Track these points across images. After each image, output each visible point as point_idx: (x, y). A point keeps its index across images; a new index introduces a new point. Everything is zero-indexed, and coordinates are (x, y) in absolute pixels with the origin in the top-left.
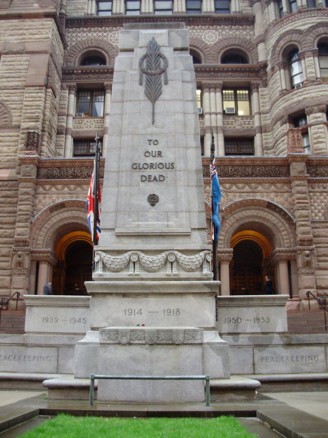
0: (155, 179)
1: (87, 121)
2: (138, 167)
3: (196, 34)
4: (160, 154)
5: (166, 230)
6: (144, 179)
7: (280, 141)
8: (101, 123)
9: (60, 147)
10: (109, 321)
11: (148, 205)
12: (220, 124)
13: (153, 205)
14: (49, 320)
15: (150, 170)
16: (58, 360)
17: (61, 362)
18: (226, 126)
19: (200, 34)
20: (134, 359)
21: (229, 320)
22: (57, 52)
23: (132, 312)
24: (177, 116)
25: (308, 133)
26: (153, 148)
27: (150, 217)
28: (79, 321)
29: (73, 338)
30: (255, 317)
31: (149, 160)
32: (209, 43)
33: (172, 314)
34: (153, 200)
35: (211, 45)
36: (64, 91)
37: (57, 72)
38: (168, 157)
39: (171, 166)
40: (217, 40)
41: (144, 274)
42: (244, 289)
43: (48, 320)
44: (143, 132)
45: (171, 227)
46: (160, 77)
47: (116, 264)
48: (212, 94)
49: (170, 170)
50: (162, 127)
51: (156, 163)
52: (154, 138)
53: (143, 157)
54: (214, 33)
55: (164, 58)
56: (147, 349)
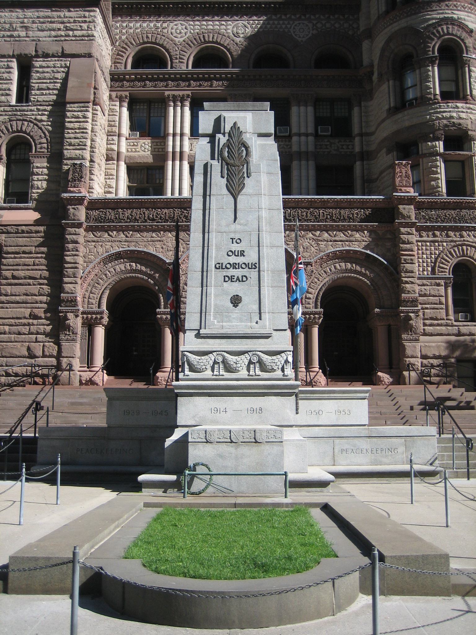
1: (144, 143)
3: (284, 26)
4: (242, 253)
5: (249, 331)
7: (385, 173)
8: (161, 145)
9: (111, 177)
12: (311, 148)
18: (318, 150)
19: (289, 26)
20: (221, 456)
21: (310, 412)
22: (103, 53)
25: (419, 165)
26: (235, 247)
27: (234, 318)
30: (336, 409)
31: (233, 259)
32: (300, 39)
33: (255, 412)
35: (302, 41)
36: (114, 103)
37: (105, 79)
39: (253, 267)
40: (310, 35)
42: (336, 353)
44: (226, 229)
45: (254, 328)
48: (302, 109)
50: (246, 225)
51: (239, 263)
54: (307, 25)
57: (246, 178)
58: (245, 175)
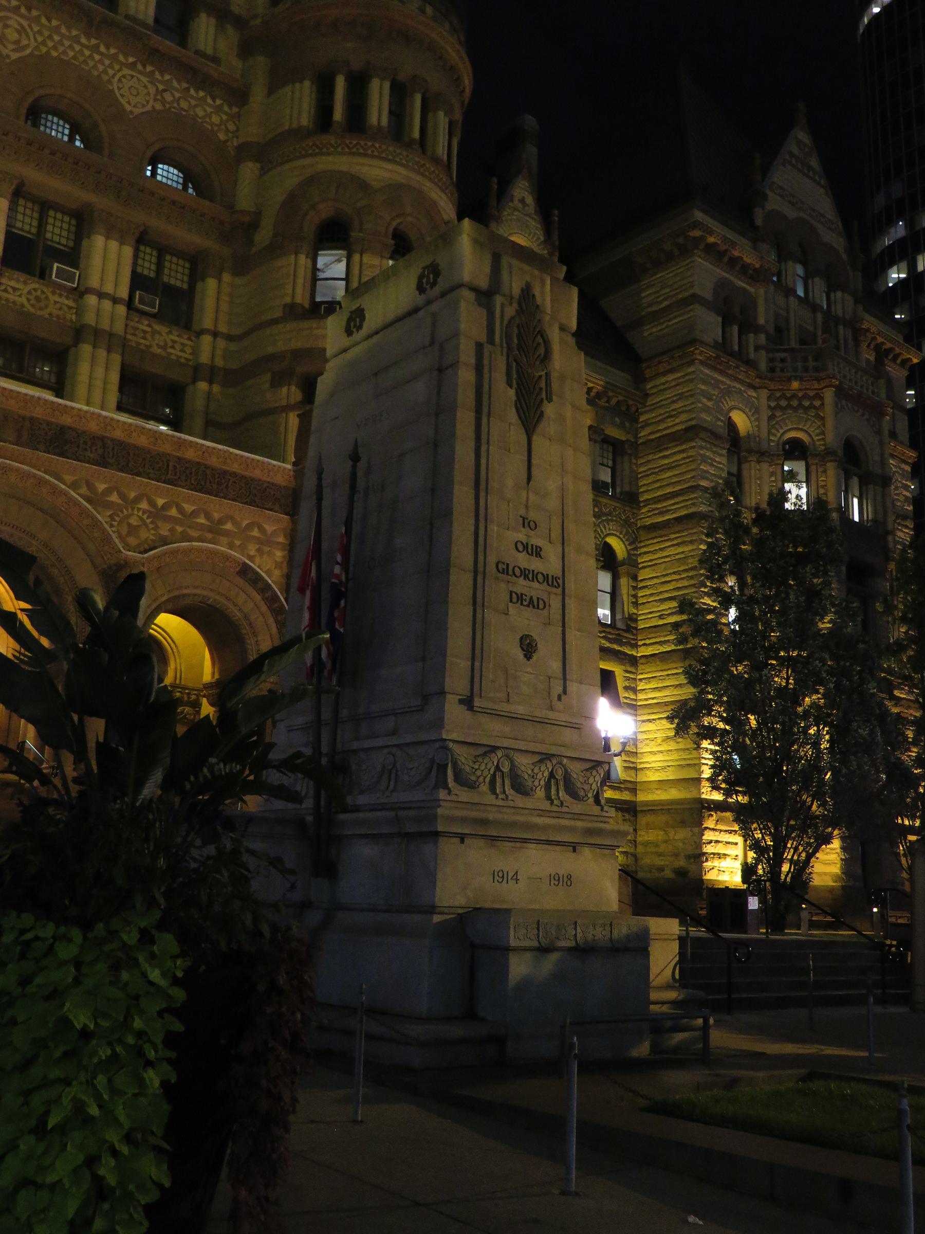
11: (520, 655)
12: (119, 328)
23: (503, 877)
32: (128, 108)
34: (528, 647)
35: (131, 112)
39: (555, 583)
40: (148, 108)
48: (113, 245)
54: (145, 87)
57: (545, 402)
58: (544, 395)
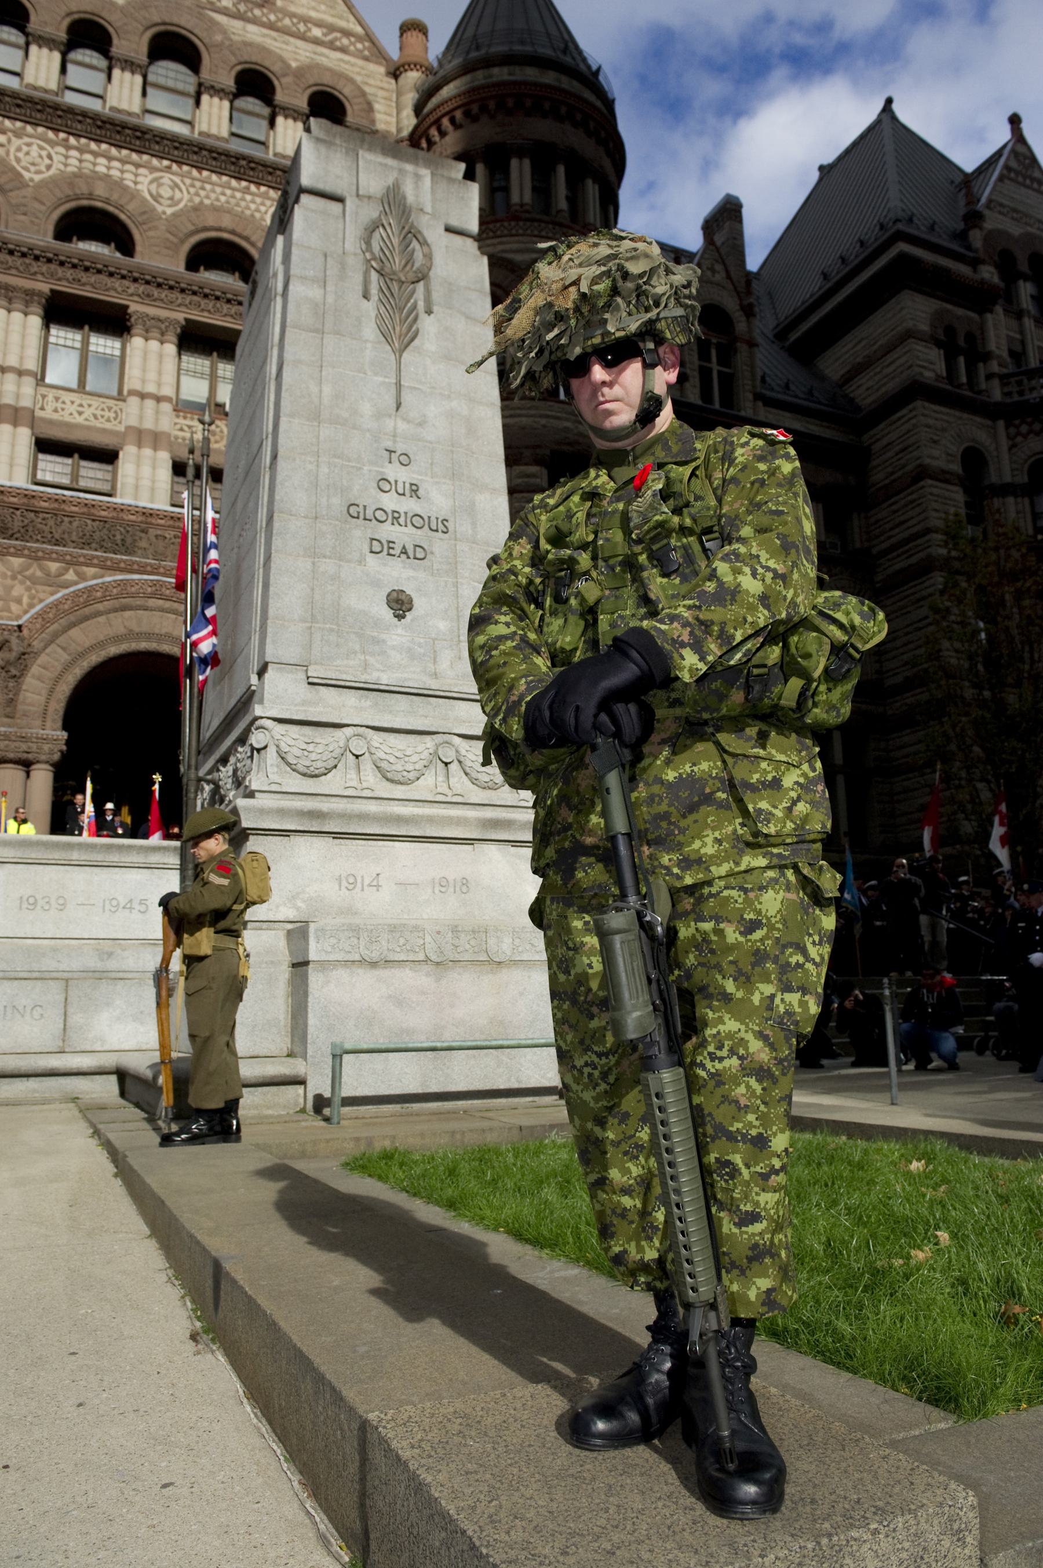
0: (404, 551)
2: (362, 516)
3: (253, 206)
6: (377, 547)
10: (300, 904)
11: (387, 614)
13: (400, 617)
14: (40, 903)
15: (392, 528)
16: (65, 1014)
17: (76, 1018)
19: (263, 209)
24: (454, 404)
27: (393, 648)
28: (129, 907)
29: (110, 954)
31: (390, 502)
34: (400, 604)
38: (438, 500)
41: (385, 789)
43: (35, 904)
46: (413, 292)
47: (313, 756)
49: (440, 534)
50: (420, 424)
52: (400, 448)
53: (374, 491)
55: (424, 243)
56: (428, 975)
57: (423, 315)
